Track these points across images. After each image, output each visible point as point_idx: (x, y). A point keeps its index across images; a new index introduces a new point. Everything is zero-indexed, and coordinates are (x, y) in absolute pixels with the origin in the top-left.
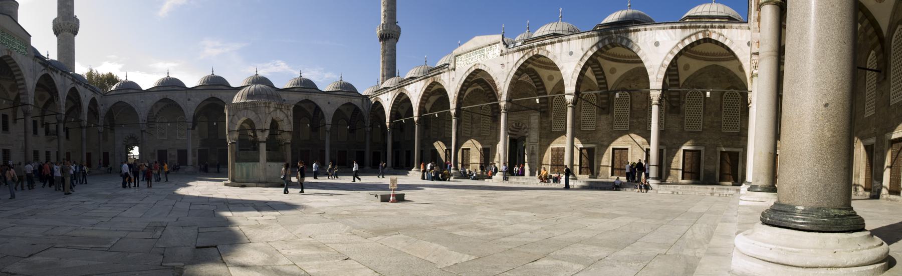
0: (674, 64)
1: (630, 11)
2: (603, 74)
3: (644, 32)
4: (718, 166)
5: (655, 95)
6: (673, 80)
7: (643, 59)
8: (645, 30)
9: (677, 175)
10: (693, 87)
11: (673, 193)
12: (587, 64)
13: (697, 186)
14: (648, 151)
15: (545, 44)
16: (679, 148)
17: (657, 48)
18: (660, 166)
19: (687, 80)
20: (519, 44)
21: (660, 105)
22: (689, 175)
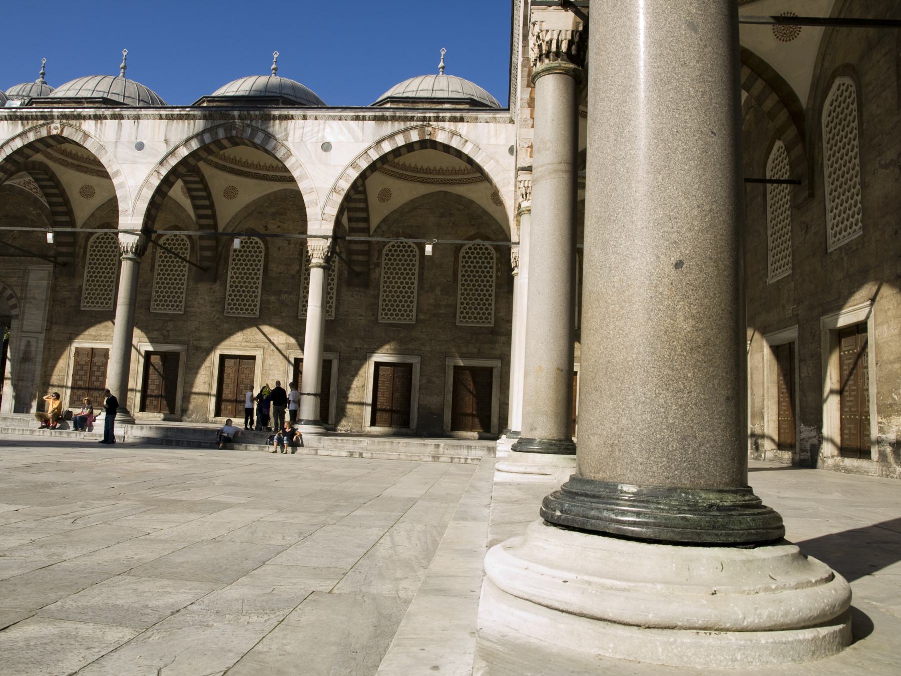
0: (358, 188)
1: (275, 80)
2: (209, 197)
3: (301, 122)
4: (449, 398)
5: (318, 249)
6: (358, 220)
7: (296, 174)
8: (305, 118)
9: (361, 416)
10: (397, 235)
11: (351, 454)
12: (174, 172)
13: (403, 441)
14: (298, 363)
15: (79, 117)
16: (365, 359)
17: (325, 156)
18: (323, 395)
19: (384, 221)
20: (17, 103)
21: (327, 267)
22: (386, 416)
